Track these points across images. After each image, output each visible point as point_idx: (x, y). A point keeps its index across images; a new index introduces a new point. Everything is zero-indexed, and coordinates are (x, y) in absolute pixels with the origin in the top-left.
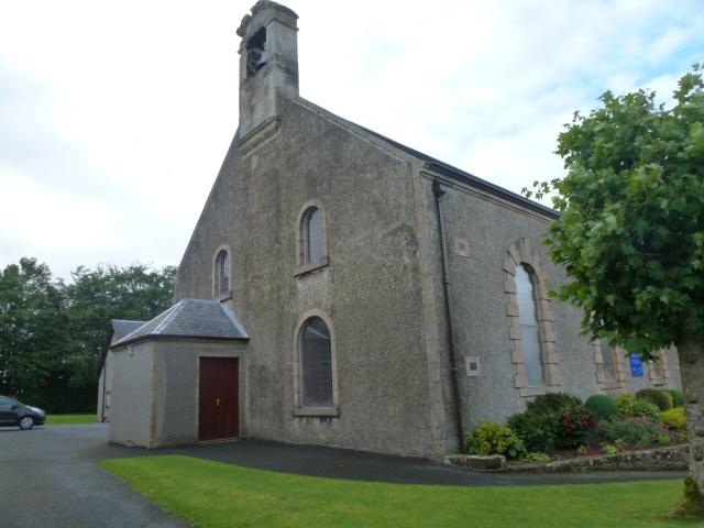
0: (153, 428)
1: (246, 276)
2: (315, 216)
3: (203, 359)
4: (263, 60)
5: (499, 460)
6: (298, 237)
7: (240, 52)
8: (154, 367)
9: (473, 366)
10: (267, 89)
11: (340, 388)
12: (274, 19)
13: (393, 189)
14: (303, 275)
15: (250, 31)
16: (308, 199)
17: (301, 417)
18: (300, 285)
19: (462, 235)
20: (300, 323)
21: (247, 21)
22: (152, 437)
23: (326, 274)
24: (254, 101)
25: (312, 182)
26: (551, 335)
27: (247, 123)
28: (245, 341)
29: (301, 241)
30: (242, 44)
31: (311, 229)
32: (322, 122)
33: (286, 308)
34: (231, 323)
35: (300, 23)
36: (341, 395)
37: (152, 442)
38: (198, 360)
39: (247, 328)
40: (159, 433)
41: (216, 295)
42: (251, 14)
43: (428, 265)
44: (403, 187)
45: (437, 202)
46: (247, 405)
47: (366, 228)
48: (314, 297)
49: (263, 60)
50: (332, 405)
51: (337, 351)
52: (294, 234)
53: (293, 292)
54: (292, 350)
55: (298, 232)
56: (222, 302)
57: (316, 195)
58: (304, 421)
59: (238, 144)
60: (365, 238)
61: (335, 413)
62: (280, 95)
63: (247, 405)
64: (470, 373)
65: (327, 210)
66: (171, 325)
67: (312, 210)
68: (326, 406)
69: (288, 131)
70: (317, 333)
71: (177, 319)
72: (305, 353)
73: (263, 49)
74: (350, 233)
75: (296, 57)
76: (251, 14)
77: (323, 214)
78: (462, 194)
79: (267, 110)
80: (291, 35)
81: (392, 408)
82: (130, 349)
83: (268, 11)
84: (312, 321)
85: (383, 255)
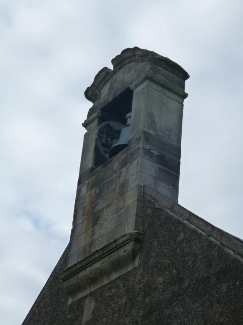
4: (122, 140)
7: (85, 125)
10: (124, 186)
15: (106, 94)
21: (103, 76)
24: (101, 204)
27: (83, 240)
30: (91, 111)
35: (189, 86)
42: (111, 67)
49: (122, 140)
62: (144, 200)
69: (152, 262)
73: (124, 122)
76: (111, 67)
79: (120, 222)
80: (173, 104)
83: (140, 65)
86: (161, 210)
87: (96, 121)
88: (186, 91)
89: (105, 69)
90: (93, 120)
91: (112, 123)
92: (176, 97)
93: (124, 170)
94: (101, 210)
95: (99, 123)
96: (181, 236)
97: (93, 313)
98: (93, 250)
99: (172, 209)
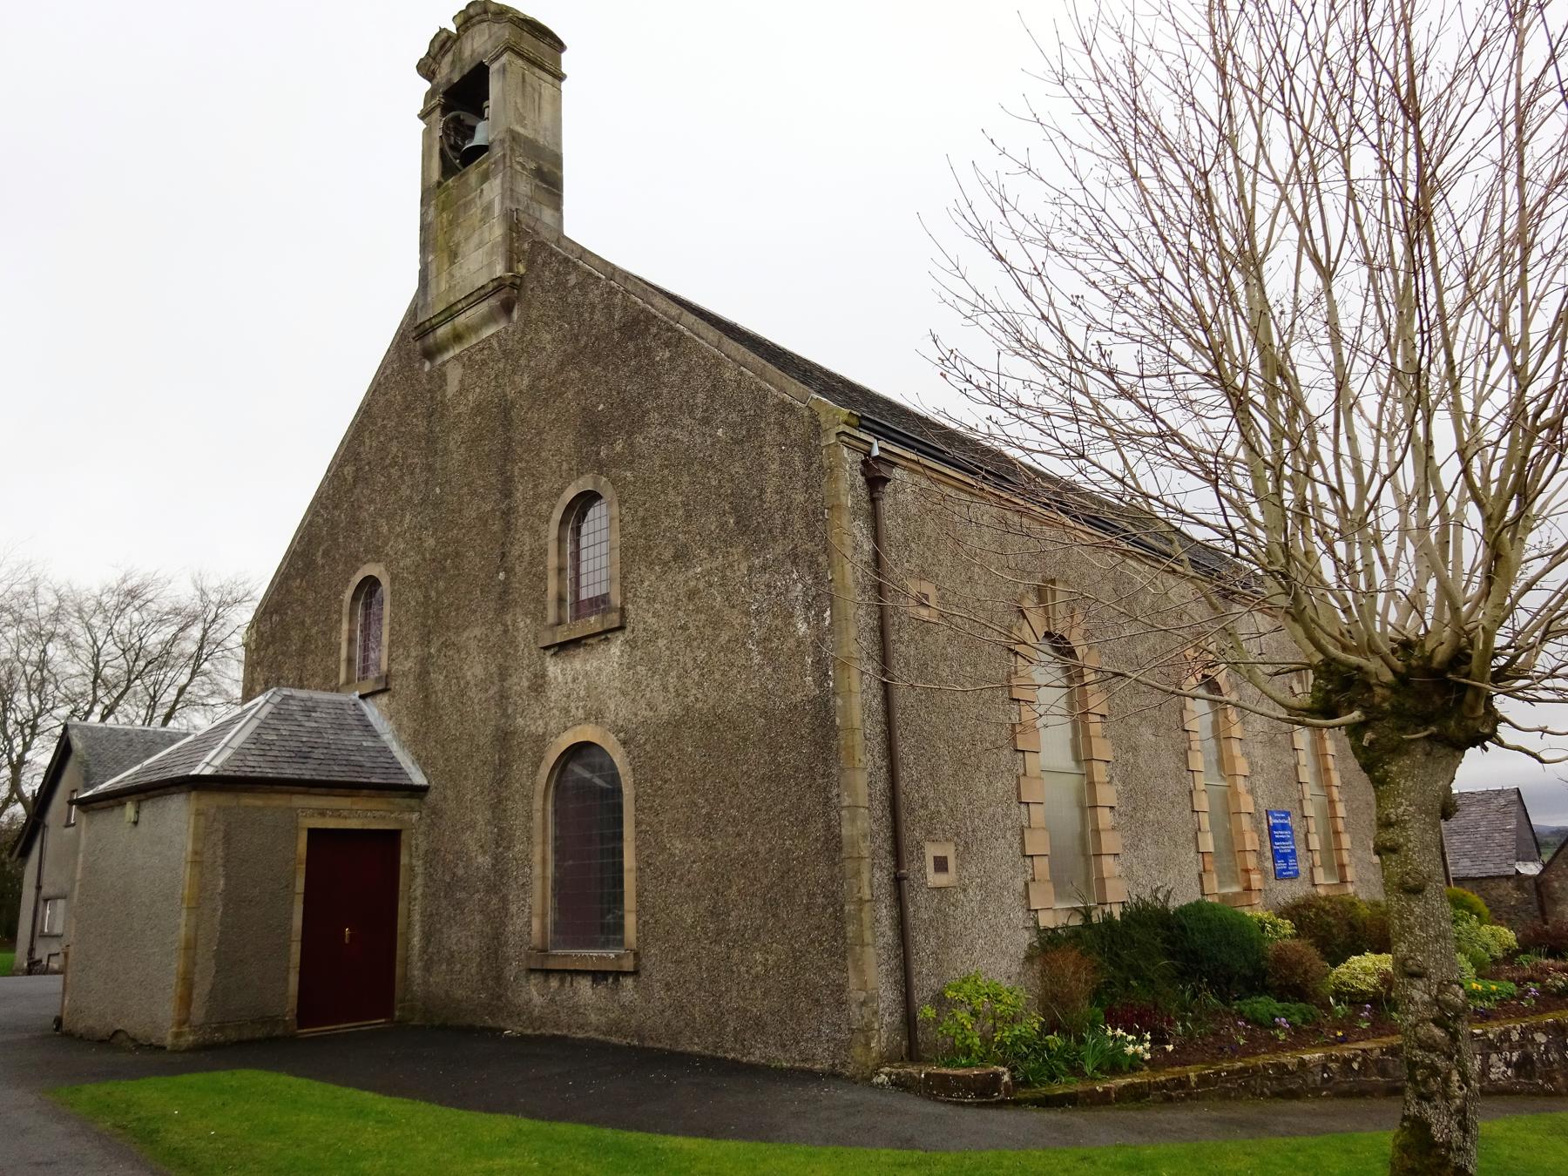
0: (186, 1001)
1: (426, 640)
2: (597, 513)
3: (317, 837)
4: (479, 139)
5: (997, 1076)
6: (552, 561)
7: (424, 116)
8: (195, 853)
9: (941, 865)
10: (488, 209)
11: (641, 908)
12: (509, 48)
13: (774, 467)
14: (563, 648)
15: (447, 72)
16: (580, 474)
17: (547, 973)
18: (554, 668)
19: (924, 575)
20: (552, 756)
21: (443, 44)
22: (181, 1023)
23: (616, 648)
24: (459, 234)
25: (593, 429)
26: (1107, 795)
28: (418, 792)
29: (561, 570)
30: (430, 95)
31: (584, 542)
32: (618, 299)
33: (520, 721)
34: (385, 750)
35: (567, 62)
36: (642, 926)
37: (177, 1035)
38: (304, 836)
39: (424, 763)
40: (198, 1013)
41: (349, 681)
42: (453, 28)
43: (855, 641)
44: (799, 465)
45: (873, 501)
46: (416, 941)
47: (712, 551)
48: (591, 697)
49: (479, 139)
50: (621, 943)
51: (638, 824)
52: (544, 552)
53: (539, 684)
54: (530, 818)
55: (552, 548)
56: (362, 697)
57: (601, 467)
58: (554, 983)
59: (419, 338)
60: (709, 572)
61: (628, 965)
62: (514, 227)
63: (416, 941)
64: (934, 879)
65: (622, 502)
66: (241, 752)
67: (587, 499)
68: (605, 945)
69: (534, 314)
70: (587, 775)
71: (256, 738)
72: (559, 824)
73: (481, 115)
74: (676, 558)
75: (559, 144)
76: (453, 28)
77: (615, 510)
78: (925, 484)
81: (758, 956)
82: (129, 810)
84: (579, 750)
85: (747, 613)
86: (543, 244)
87: (438, 111)
88: (564, 70)
89: (442, 30)
90: (433, 110)
91: (463, 115)
92: (549, 78)
93: (485, 186)
94: (458, 245)
95: (444, 114)
96: (573, 280)
97: (461, 381)
98: (453, 300)
99: (558, 243)
